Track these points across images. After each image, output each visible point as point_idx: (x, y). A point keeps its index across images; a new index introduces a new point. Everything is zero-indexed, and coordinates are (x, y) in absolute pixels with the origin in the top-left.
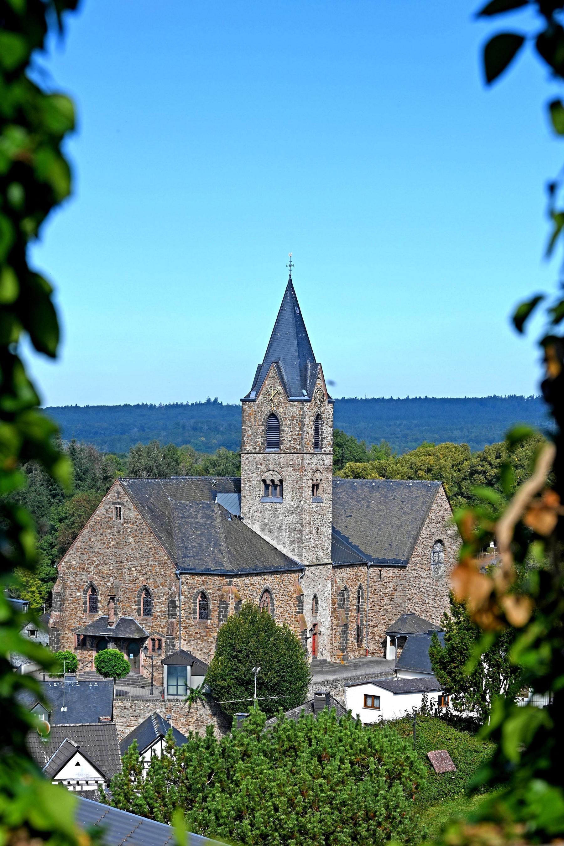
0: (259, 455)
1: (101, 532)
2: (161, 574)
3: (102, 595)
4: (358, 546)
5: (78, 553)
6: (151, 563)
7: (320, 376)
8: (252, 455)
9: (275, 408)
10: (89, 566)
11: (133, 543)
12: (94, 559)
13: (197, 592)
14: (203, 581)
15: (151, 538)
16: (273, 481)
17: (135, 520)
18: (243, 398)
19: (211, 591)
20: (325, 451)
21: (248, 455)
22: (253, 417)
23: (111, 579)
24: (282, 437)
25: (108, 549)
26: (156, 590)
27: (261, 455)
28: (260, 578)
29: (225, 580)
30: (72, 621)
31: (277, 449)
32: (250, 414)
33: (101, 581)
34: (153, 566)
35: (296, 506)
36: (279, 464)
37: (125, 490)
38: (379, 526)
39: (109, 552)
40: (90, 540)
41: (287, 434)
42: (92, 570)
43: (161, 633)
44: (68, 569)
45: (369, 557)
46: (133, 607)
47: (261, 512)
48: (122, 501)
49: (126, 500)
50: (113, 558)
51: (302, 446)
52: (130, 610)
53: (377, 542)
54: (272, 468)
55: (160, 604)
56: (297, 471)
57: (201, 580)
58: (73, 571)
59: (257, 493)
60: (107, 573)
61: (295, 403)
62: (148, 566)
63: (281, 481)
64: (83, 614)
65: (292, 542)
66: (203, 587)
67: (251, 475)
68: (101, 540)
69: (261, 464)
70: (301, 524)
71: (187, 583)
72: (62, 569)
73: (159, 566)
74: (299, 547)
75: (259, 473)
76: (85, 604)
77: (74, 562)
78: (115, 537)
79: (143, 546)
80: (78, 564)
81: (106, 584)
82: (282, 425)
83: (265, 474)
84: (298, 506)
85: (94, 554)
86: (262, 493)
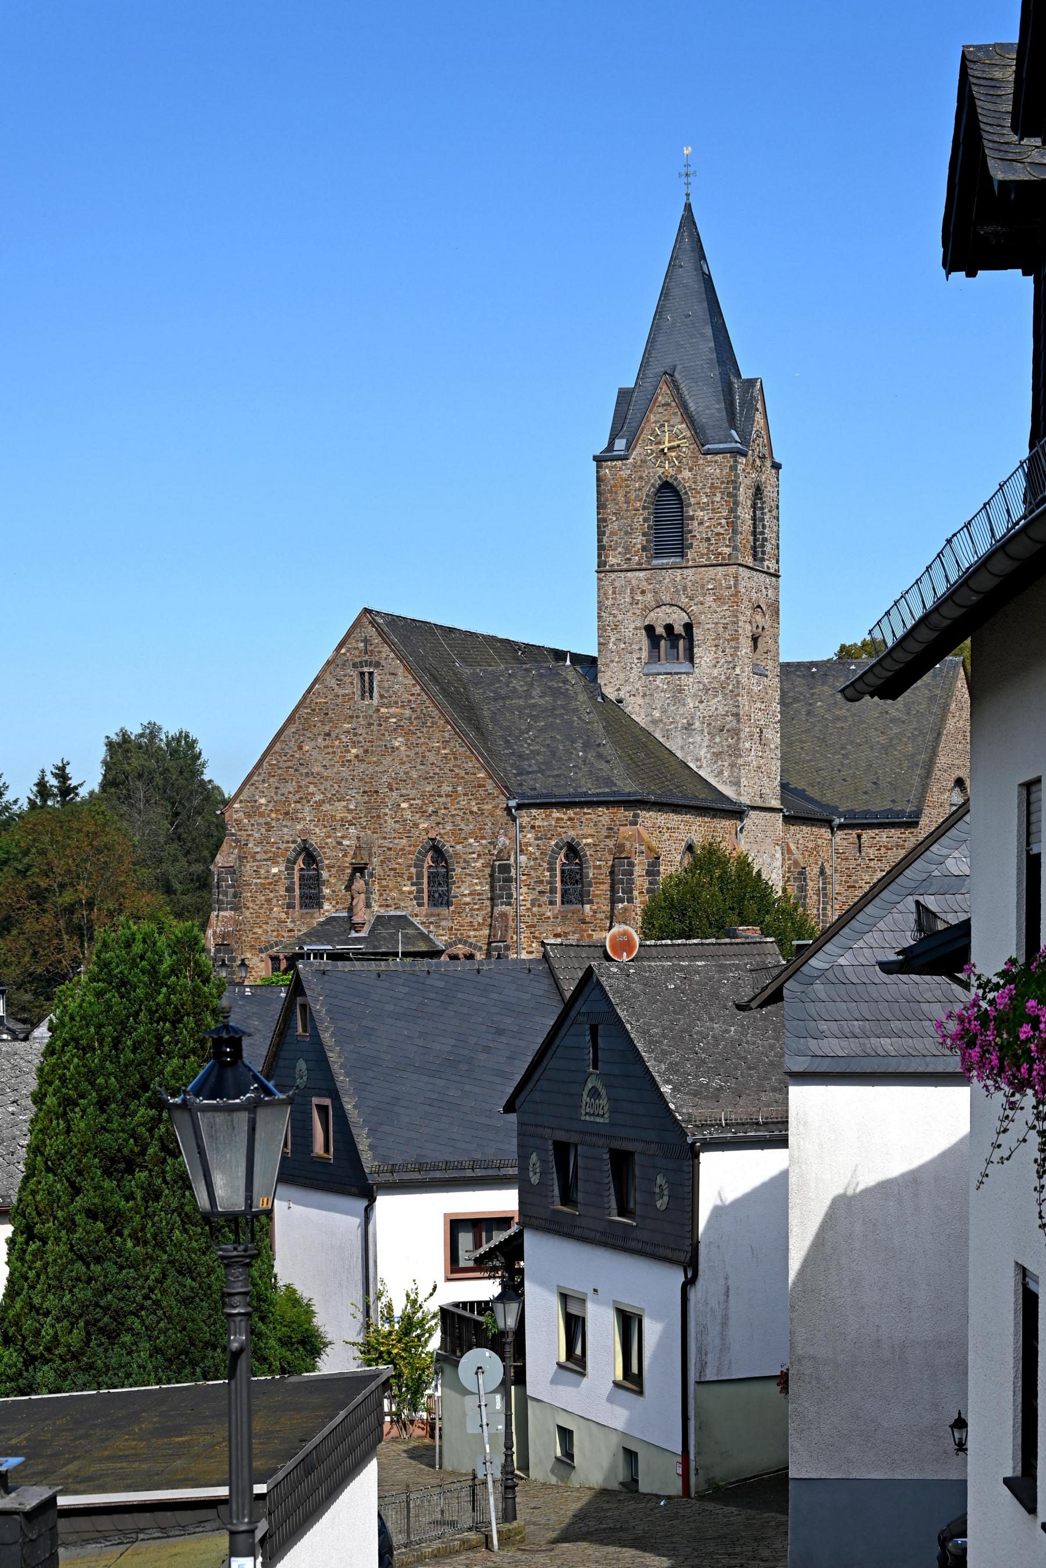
0: (637, 574)
1: (327, 729)
2: (471, 812)
4: (804, 790)
5: (272, 780)
6: (446, 788)
7: (759, 406)
8: (622, 574)
9: (672, 471)
10: (299, 806)
11: (403, 749)
12: (312, 789)
13: (556, 845)
14: (570, 819)
15: (446, 735)
16: (669, 628)
17: (406, 697)
18: (598, 453)
19: (590, 841)
20: (768, 568)
21: (613, 575)
22: (621, 493)
23: (352, 830)
24: (690, 531)
25: (343, 766)
26: (459, 847)
27: (642, 574)
28: (680, 817)
29: (622, 814)
30: (259, 931)
31: (678, 560)
32: (615, 486)
33: (329, 837)
34: (452, 795)
35: (723, 677)
36: (685, 589)
37: (381, 633)
38: (842, 748)
39: (345, 772)
40: (300, 748)
41: (701, 523)
42: (307, 813)
43: (473, 940)
44: (248, 816)
45: (834, 811)
46: (404, 889)
47: (644, 696)
48: (375, 659)
49: (384, 655)
50: (356, 783)
51: (735, 548)
52: (396, 895)
53: (844, 780)
54: (668, 600)
55: (469, 878)
56: (724, 603)
57: (565, 817)
58: (262, 820)
59: (635, 656)
60: (342, 819)
61: (718, 458)
62: (440, 796)
63: (688, 627)
64: (287, 913)
65: (717, 755)
66: (572, 833)
67: (620, 617)
68: (327, 747)
69: (643, 592)
70: (737, 715)
71: (533, 827)
72: (235, 816)
73: (465, 795)
74: (732, 765)
75: (638, 612)
76: (290, 889)
77: (263, 801)
78: (361, 739)
79: (427, 754)
80: (271, 805)
81: (341, 844)
82: (689, 505)
83: (652, 614)
84: (728, 678)
85: (310, 779)
86: (644, 654)
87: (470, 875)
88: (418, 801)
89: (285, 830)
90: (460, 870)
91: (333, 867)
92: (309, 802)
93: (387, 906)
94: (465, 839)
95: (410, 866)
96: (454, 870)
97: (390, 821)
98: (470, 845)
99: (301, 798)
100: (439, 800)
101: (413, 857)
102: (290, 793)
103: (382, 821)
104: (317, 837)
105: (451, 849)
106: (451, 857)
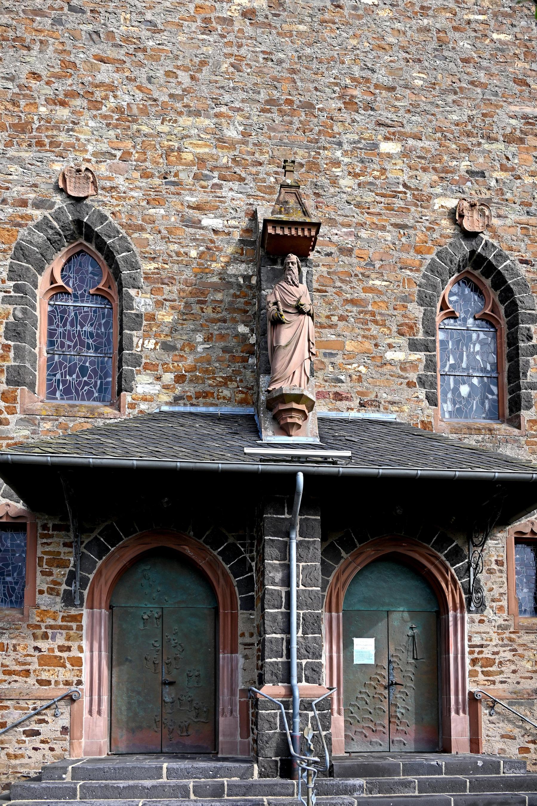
3: (156, 280)
10: (63, 113)
12: (106, 74)
25: (207, 30)
46: (390, 355)
60: (201, 161)
79: (452, 34)
81: (196, 224)
88: (426, 144)
92: (96, 105)
93: (338, 397)
95: (406, 299)
97: (346, 182)
99: (73, 94)
100: (486, 146)
101: (417, 276)
102: (36, 76)
103: (323, 180)
104: (120, 200)
105: (522, 269)
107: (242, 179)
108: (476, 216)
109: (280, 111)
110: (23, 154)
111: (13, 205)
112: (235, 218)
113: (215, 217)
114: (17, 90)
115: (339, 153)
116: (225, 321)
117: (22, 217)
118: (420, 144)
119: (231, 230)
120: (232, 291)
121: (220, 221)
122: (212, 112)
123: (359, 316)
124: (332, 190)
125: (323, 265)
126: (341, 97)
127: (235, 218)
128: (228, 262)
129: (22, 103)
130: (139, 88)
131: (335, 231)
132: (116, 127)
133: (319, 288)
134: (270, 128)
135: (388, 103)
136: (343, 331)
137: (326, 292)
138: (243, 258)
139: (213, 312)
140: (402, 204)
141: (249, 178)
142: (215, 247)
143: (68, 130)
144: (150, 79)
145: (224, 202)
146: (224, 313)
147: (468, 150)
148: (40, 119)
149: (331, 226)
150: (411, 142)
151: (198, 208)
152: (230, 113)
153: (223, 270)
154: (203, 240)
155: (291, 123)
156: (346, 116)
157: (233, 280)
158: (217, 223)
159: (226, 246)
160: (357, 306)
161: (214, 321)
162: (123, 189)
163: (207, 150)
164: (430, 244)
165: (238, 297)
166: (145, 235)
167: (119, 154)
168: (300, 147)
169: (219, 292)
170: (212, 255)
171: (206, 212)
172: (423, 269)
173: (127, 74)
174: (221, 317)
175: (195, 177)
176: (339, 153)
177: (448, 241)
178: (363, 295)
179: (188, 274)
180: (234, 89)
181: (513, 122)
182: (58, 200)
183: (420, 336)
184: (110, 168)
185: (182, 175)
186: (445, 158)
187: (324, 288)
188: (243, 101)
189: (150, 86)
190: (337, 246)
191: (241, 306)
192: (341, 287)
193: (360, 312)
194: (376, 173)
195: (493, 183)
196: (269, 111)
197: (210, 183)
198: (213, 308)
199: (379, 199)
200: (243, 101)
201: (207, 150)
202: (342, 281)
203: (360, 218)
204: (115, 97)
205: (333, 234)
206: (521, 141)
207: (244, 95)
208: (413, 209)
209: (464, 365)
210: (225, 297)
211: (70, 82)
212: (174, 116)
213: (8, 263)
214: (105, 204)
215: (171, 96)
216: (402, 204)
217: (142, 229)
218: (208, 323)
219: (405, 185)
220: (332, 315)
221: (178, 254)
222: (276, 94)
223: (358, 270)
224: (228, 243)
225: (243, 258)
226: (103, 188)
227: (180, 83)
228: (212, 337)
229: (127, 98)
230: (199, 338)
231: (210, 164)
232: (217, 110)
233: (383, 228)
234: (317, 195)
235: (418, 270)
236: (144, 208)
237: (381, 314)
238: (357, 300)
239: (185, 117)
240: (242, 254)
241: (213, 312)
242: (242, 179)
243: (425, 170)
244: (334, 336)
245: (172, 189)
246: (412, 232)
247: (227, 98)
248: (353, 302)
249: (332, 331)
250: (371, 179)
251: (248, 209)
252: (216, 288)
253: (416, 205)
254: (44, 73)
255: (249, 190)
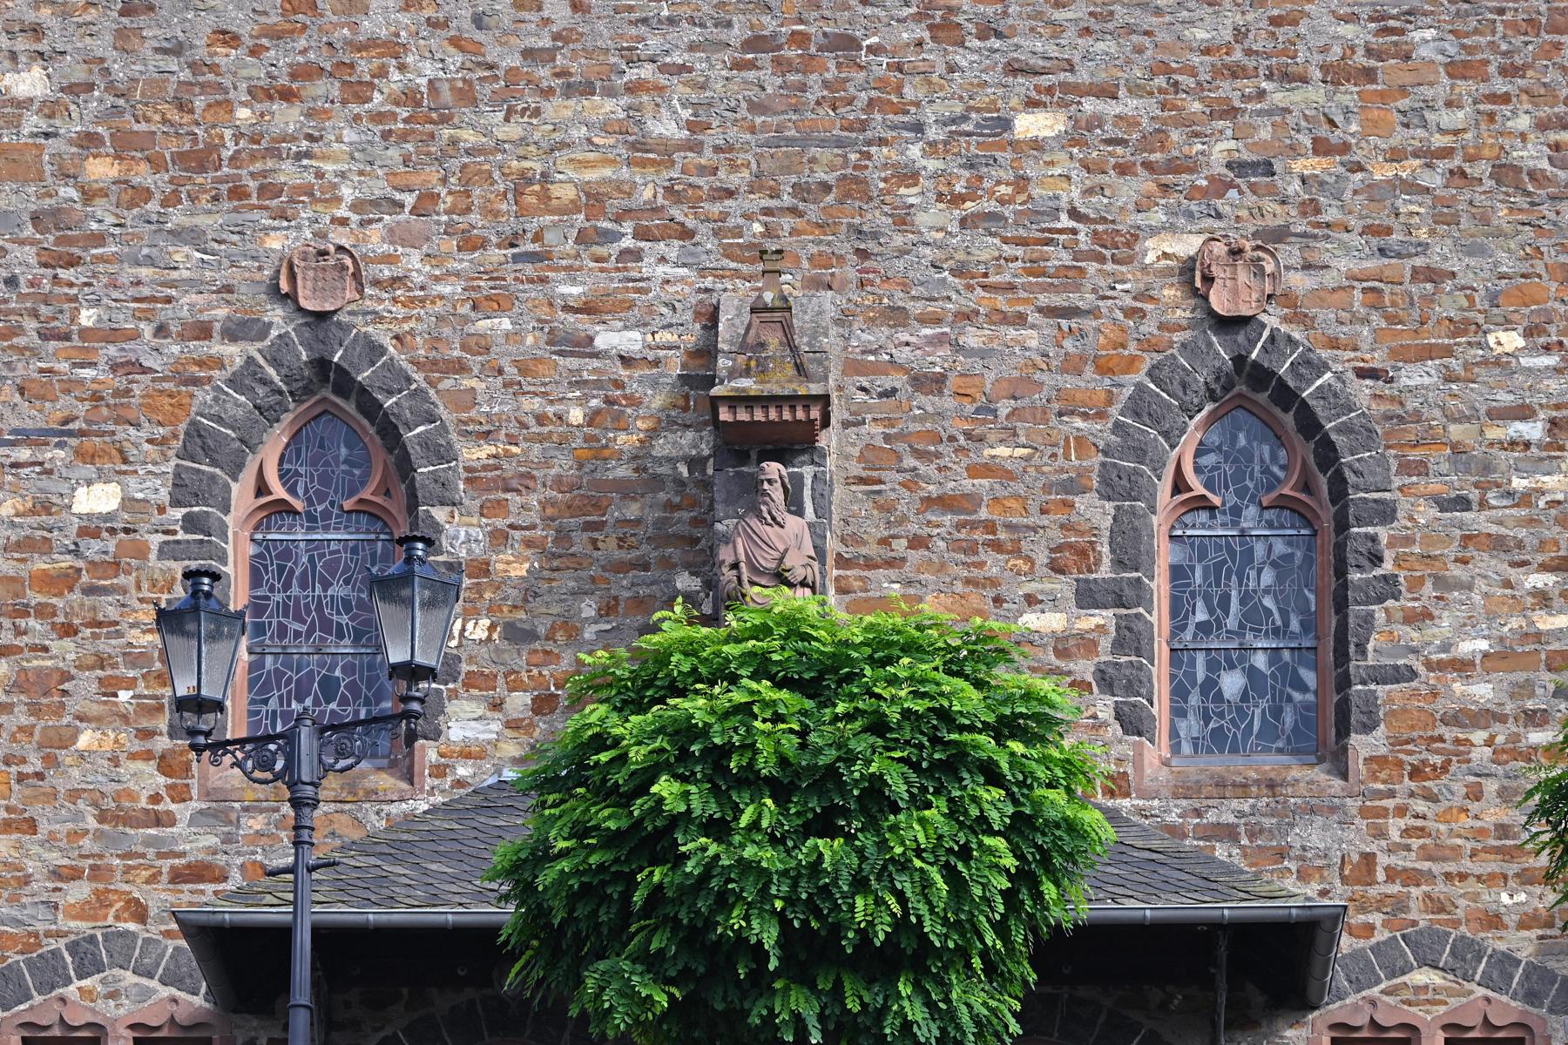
2: (1505, 173)
3: (491, 484)
10: (288, 117)
23: (663, 267)
26: (1413, 376)
33: (498, 303)
42: (347, 158)
55: (1489, 565)
60: (593, 199)
62: (1287, 77)
73: (1457, 70)
80: (96, 102)
81: (583, 346)
87: (1497, 544)
88: (1129, 105)
89: (185, 255)
90: (1426, 514)
91: (526, 482)
92: (358, 92)
94: (1459, 328)
95: (1074, 486)
96: (1386, 513)
97: (931, 217)
98: (1500, 363)
100: (1279, 97)
102: (228, 38)
106: (1364, 434)
107: (686, 234)
108: (1243, 276)
109: (777, 62)
110: (202, 221)
111: (182, 337)
112: (670, 325)
113: (626, 328)
114: (186, 75)
115: (915, 151)
116: (646, 567)
117: (200, 364)
118: (1111, 109)
119: (662, 353)
120: (662, 496)
121: (636, 335)
122: (620, 82)
123: (957, 535)
124: (899, 240)
125: (874, 420)
126: (919, 17)
127: (670, 325)
128: (654, 430)
129: (199, 103)
130: (456, 42)
131: (905, 337)
132: (404, 137)
133: (864, 474)
134: (754, 107)
135: (1038, 16)
136: (918, 571)
137: (881, 482)
138: (690, 417)
139: (620, 547)
140: (1066, 258)
141: (704, 229)
142: (625, 397)
143: (299, 156)
144: (478, 21)
145: (646, 291)
146: (645, 548)
147: (1231, 112)
148: (237, 137)
149: (895, 326)
150: (1090, 105)
151: (588, 309)
152: (662, 80)
153: (641, 448)
154: (598, 384)
155: (803, 88)
156: (933, 56)
157: (664, 470)
158: (630, 340)
159: (650, 392)
160: (954, 512)
161: (621, 567)
162: (419, 279)
163: (607, 172)
164: (1132, 348)
165: (678, 507)
166: (468, 383)
167: (409, 199)
168: (823, 143)
169: (633, 499)
170: (618, 416)
171: (605, 317)
172: (1114, 411)
173: (429, 12)
174: (638, 558)
175: (582, 238)
176: (915, 151)
177: (1178, 337)
178: (968, 484)
179: (563, 465)
180: (671, 21)
181: (1348, 30)
182: (276, 315)
183: (1105, 571)
184: (392, 235)
185: (549, 237)
186: (1175, 135)
187: (875, 474)
188: (692, 47)
189: (479, 36)
190: (907, 372)
191: (684, 529)
192: (915, 469)
193: (959, 526)
194: (1004, 190)
195: (1295, 186)
196: (751, 65)
197: (614, 249)
198: (620, 539)
199: (1009, 250)
200: (692, 47)
201: (607, 172)
202: (920, 455)
203: (967, 301)
204: (402, 68)
205: (901, 344)
206: (1369, 75)
207: (695, 34)
208: (1092, 267)
209: (1231, 623)
210: (647, 510)
211: (302, 43)
212: (532, 101)
213: (169, 468)
214: (378, 318)
215: (528, 53)
216: (1066, 258)
217: (461, 368)
218: (607, 575)
219: (1074, 214)
220: (894, 537)
221: (541, 419)
222: (769, 24)
223: (957, 427)
224: (655, 384)
225: (690, 417)
226: (376, 283)
227: (547, 21)
228: (617, 604)
229: (429, 69)
230: (588, 608)
231: (615, 204)
232: (632, 74)
233: (1020, 320)
234: (863, 254)
235: (1101, 415)
236: (466, 320)
237: (1010, 527)
238: (953, 498)
239: (557, 101)
240: (686, 409)
241: (620, 547)
242: (686, 234)
243: (1123, 170)
244: (896, 586)
245: (529, 269)
246: (1089, 324)
247: (654, 43)
248: (943, 503)
249: (893, 573)
250: (989, 206)
251: (701, 302)
252: (626, 490)
253: (1101, 259)
254: (245, 30)
255: (704, 257)
